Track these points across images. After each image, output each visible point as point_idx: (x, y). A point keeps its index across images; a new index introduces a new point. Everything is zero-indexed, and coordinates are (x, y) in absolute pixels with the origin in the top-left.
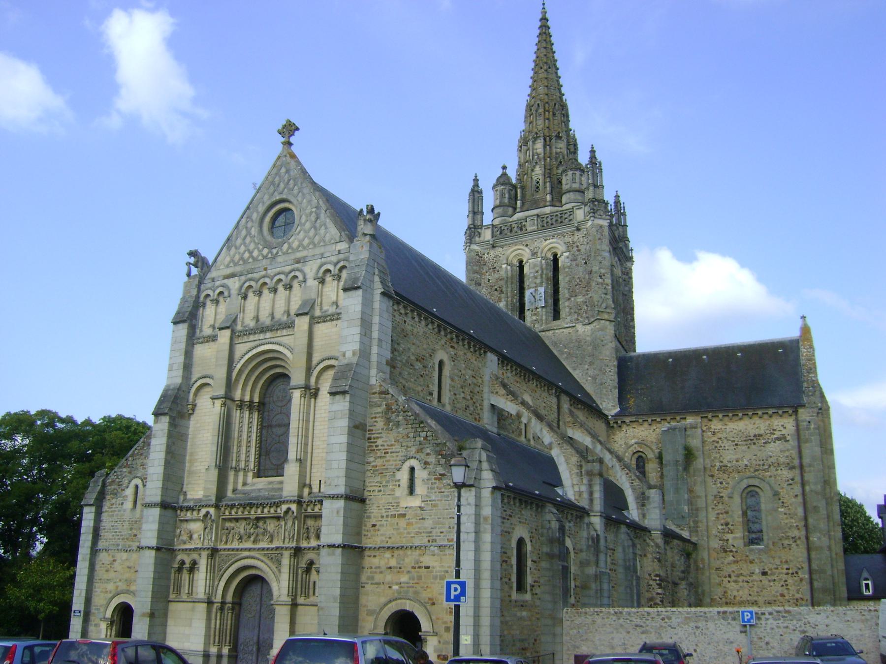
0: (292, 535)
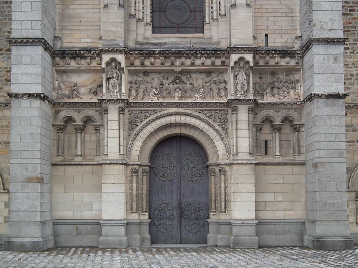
0: (246, 88)
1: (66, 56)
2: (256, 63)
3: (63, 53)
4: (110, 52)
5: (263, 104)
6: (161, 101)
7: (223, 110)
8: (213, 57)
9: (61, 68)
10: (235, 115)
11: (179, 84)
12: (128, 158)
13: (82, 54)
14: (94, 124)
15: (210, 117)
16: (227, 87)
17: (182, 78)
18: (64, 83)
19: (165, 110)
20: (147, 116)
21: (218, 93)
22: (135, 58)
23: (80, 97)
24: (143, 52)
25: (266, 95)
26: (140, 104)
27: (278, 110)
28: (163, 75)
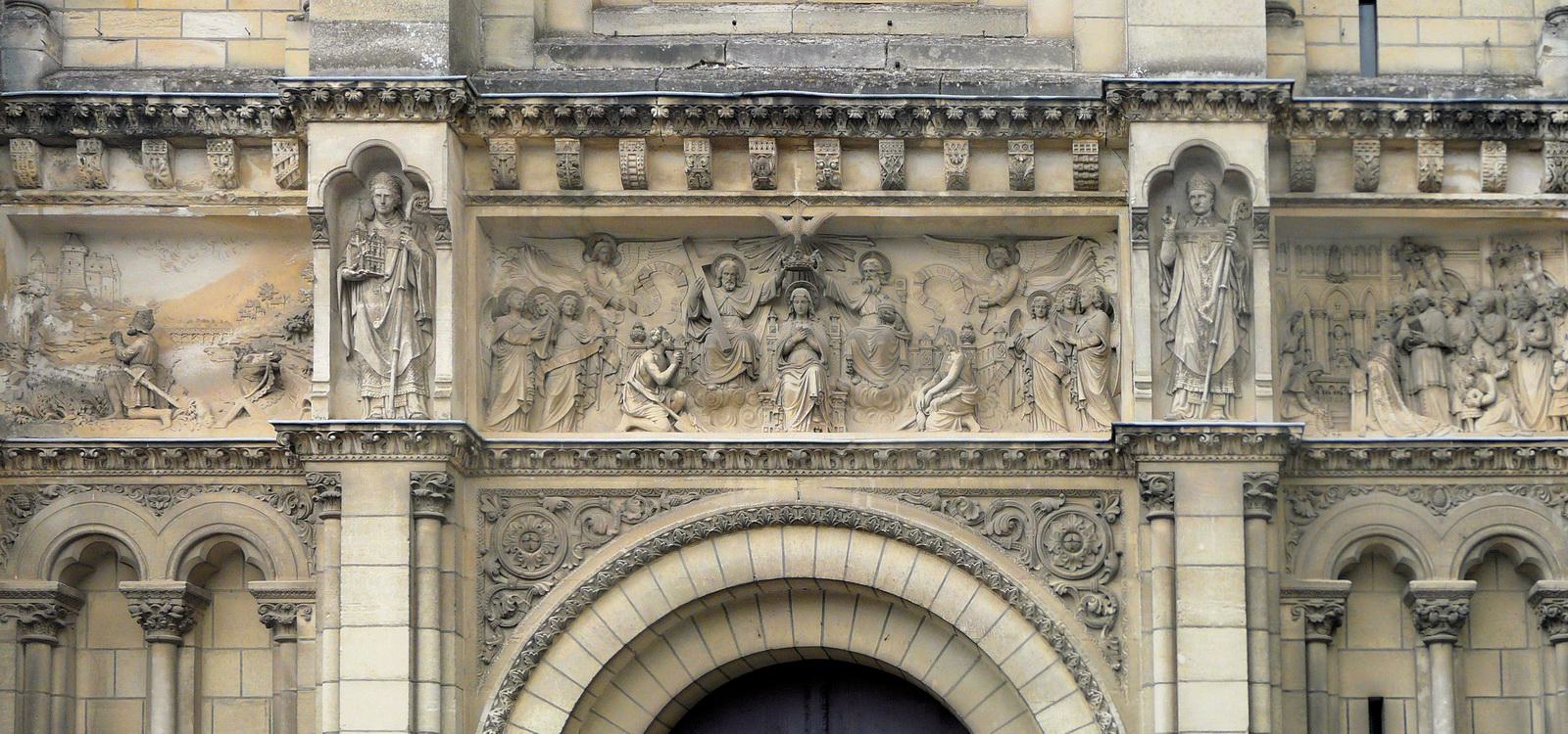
1: (75, 131)
2: (1299, 187)
3: (57, 115)
4: (357, 105)
5: (1344, 454)
6: (691, 430)
7: (1092, 494)
8: (1020, 142)
9: (50, 211)
10: (1161, 526)
11: (808, 314)
13: (184, 120)
14: (256, 585)
15: (1010, 536)
16: (1115, 341)
17: (828, 277)
18: (67, 306)
19: (718, 491)
20: (597, 533)
21: (1060, 382)
22: (524, 146)
23: (171, 406)
24: (572, 108)
25: (1367, 392)
26: (554, 450)
27: (1438, 496)
28: (708, 255)
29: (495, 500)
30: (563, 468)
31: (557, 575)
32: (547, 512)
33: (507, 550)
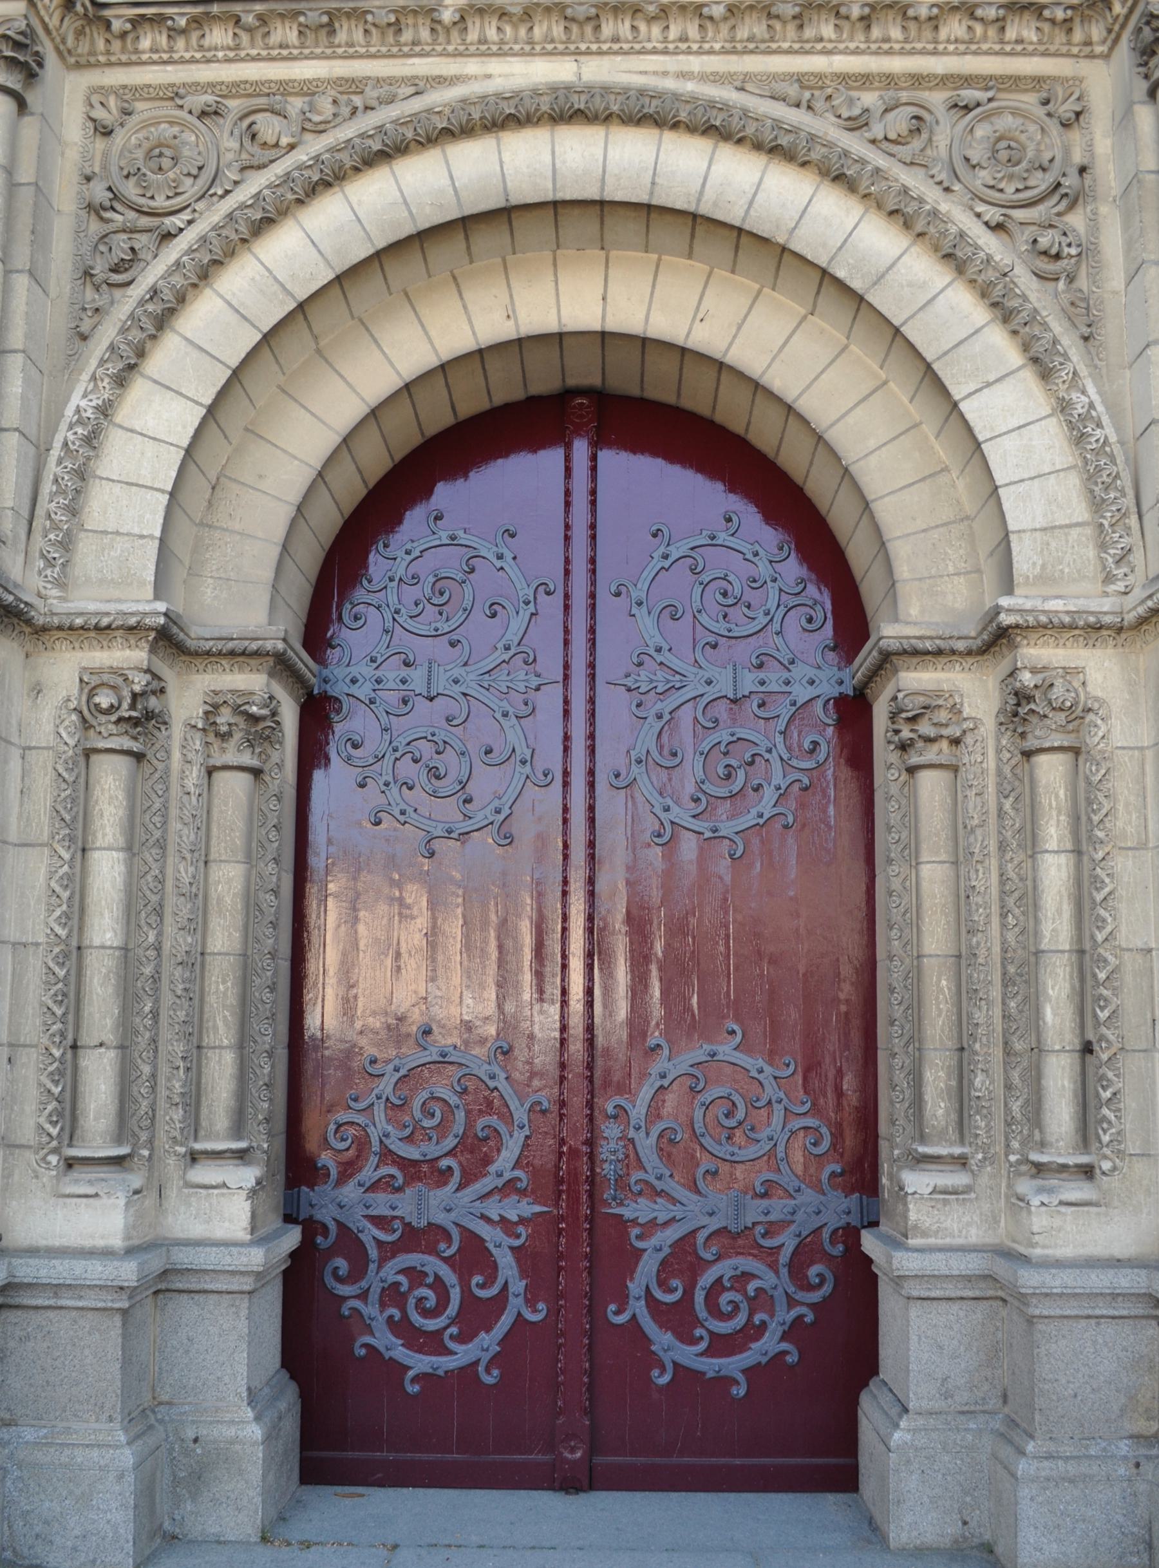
7: (1038, 81)
12: (50, 563)
29: (112, 102)
30: (216, 49)
31: (199, 206)
32: (189, 117)
33: (125, 173)
